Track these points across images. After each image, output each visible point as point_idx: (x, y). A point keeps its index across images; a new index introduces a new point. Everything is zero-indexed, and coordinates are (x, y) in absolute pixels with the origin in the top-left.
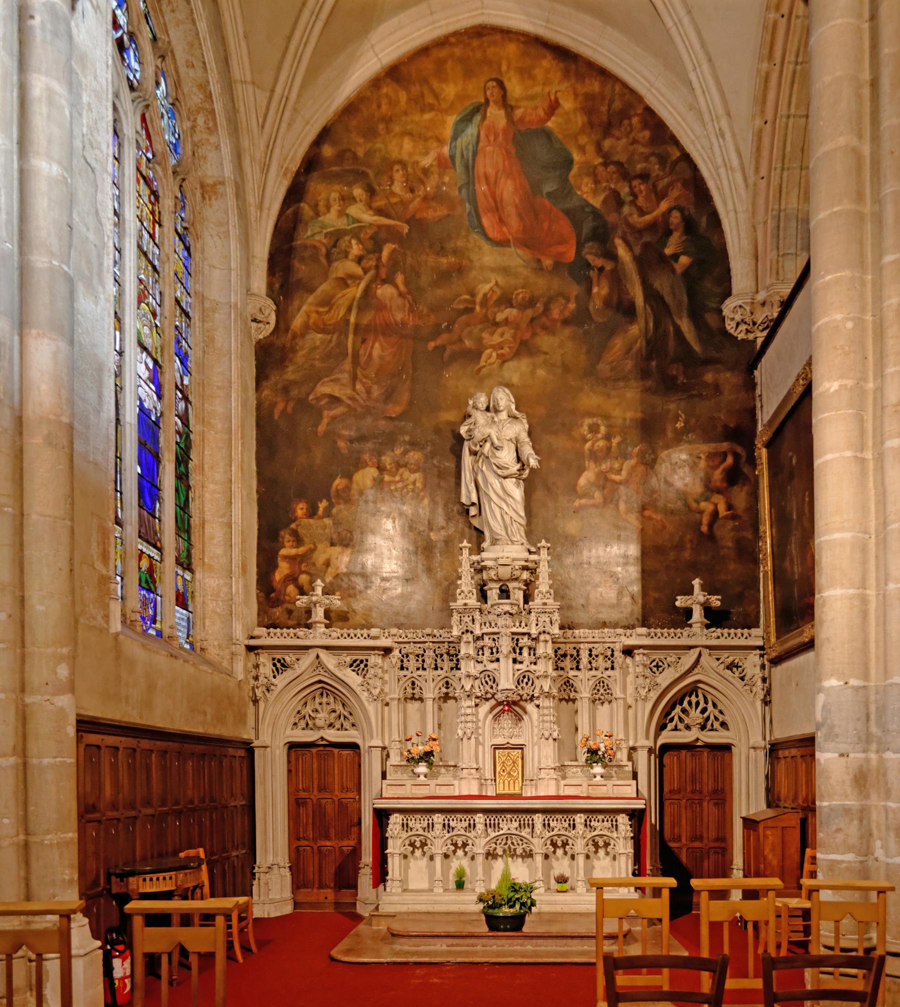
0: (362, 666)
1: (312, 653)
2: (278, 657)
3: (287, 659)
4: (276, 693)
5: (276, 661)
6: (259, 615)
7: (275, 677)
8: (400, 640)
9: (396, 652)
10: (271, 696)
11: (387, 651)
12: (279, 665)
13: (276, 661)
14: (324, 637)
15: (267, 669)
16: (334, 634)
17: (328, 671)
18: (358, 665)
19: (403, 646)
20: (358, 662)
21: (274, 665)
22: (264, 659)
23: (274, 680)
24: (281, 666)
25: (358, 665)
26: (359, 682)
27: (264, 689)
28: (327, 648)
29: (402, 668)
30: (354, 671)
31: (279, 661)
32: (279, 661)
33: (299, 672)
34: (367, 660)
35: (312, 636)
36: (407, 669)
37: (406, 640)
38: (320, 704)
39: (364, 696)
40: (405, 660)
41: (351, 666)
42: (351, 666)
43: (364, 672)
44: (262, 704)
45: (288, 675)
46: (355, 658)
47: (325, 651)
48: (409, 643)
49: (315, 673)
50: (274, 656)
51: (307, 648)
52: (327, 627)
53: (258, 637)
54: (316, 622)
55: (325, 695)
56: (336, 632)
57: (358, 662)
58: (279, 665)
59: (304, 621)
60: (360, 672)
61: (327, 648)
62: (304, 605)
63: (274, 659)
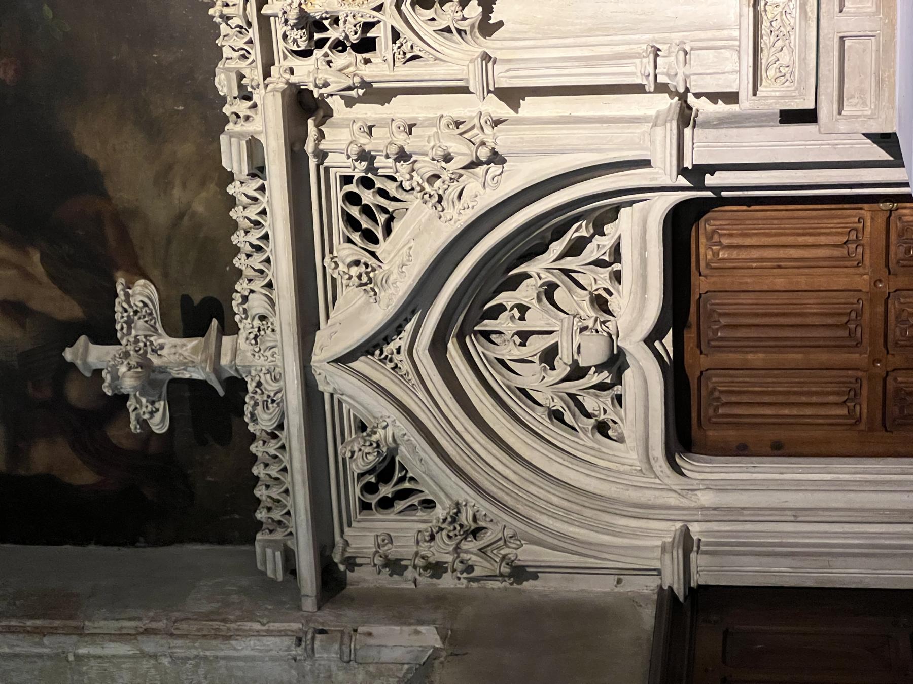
0: (368, 197)
1: (332, 381)
2: (355, 491)
3: (358, 466)
4: (484, 507)
5: (373, 499)
6: (222, 541)
7: (429, 504)
8: (256, 53)
9: (306, 72)
10: (499, 524)
11: (304, 106)
12: (386, 491)
13: (373, 499)
14: (269, 338)
15: (403, 531)
16: (257, 304)
17: (394, 327)
18: (367, 211)
19: (279, 46)
20: (355, 211)
21: (386, 504)
22: (363, 536)
23: (440, 512)
24: (388, 483)
25: (367, 211)
26: (428, 210)
27: (471, 545)
28: (308, 326)
29: (366, 45)
30: (388, 231)
31: (370, 488)
32: (370, 488)
33: (401, 426)
34: (347, 180)
35: (270, 387)
36: (368, 26)
37: (254, 33)
38: (524, 336)
39: (483, 191)
40: (333, 34)
41: (370, 236)
42: (370, 236)
43: (391, 187)
44: (528, 554)
45: (417, 458)
46: (339, 226)
47: (321, 337)
48: (264, 21)
49: (406, 366)
50: (354, 505)
51: (312, 394)
52: (229, 328)
53: (289, 557)
54: (217, 369)
55: (488, 325)
56: (249, 299)
57: (355, 211)
58: (386, 491)
59: (213, 409)
60: (390, 206)
61: (308, 326)
62: (161, 405)
63: (365, 506)
